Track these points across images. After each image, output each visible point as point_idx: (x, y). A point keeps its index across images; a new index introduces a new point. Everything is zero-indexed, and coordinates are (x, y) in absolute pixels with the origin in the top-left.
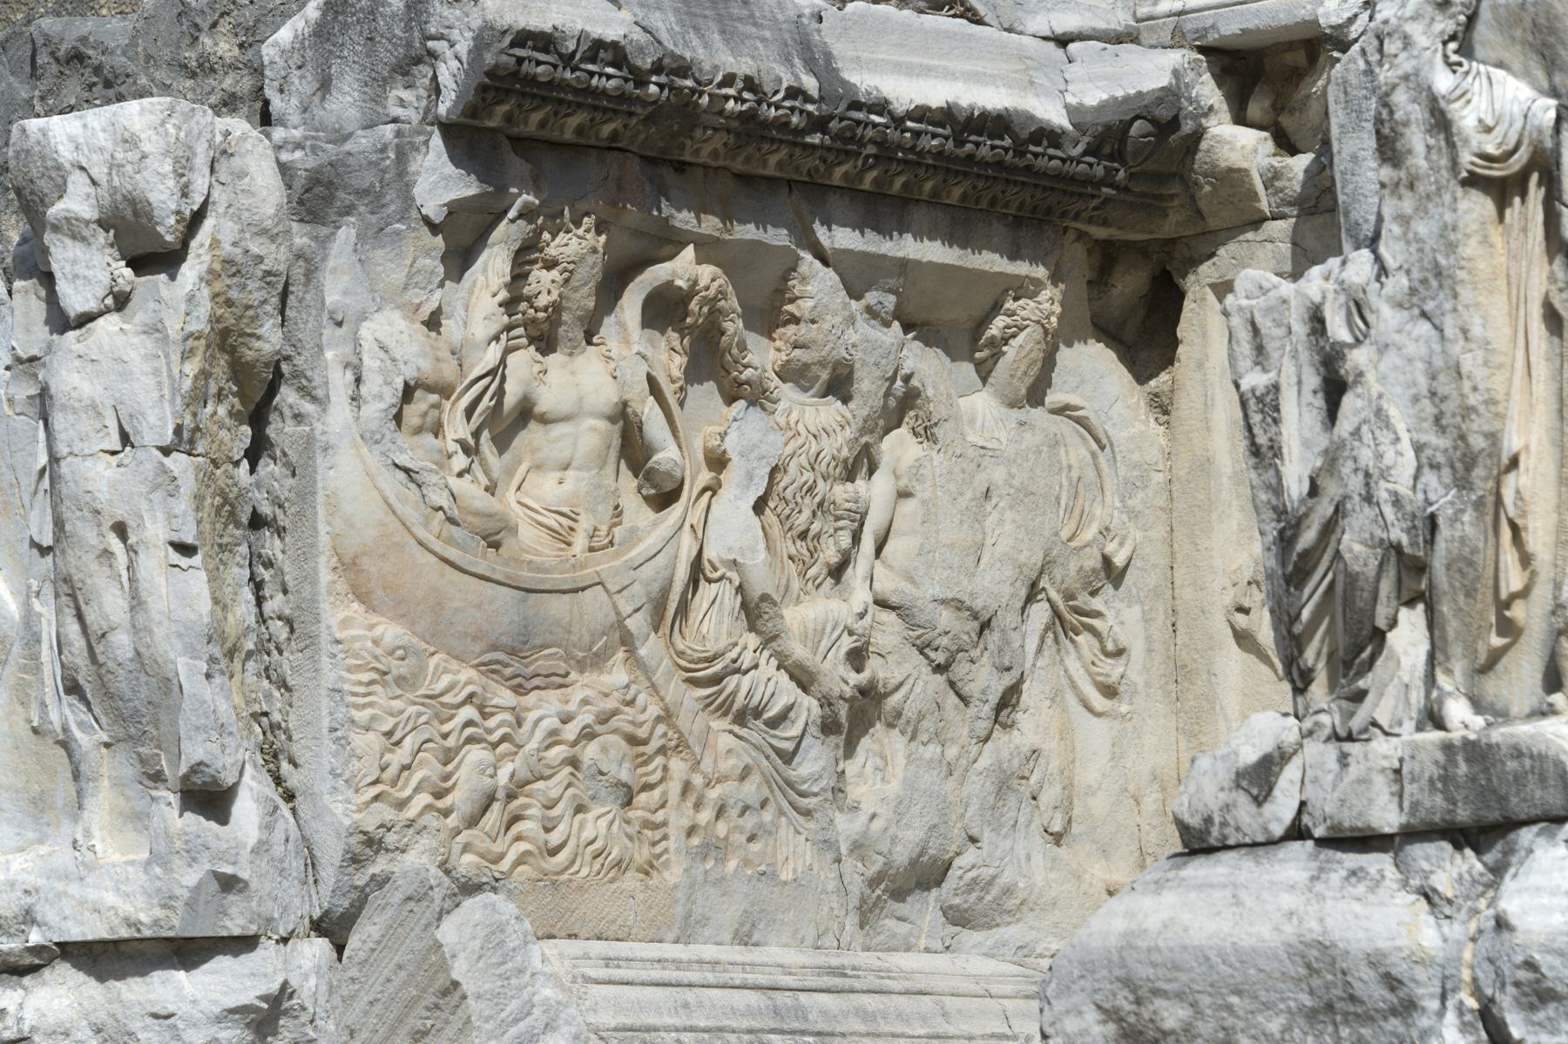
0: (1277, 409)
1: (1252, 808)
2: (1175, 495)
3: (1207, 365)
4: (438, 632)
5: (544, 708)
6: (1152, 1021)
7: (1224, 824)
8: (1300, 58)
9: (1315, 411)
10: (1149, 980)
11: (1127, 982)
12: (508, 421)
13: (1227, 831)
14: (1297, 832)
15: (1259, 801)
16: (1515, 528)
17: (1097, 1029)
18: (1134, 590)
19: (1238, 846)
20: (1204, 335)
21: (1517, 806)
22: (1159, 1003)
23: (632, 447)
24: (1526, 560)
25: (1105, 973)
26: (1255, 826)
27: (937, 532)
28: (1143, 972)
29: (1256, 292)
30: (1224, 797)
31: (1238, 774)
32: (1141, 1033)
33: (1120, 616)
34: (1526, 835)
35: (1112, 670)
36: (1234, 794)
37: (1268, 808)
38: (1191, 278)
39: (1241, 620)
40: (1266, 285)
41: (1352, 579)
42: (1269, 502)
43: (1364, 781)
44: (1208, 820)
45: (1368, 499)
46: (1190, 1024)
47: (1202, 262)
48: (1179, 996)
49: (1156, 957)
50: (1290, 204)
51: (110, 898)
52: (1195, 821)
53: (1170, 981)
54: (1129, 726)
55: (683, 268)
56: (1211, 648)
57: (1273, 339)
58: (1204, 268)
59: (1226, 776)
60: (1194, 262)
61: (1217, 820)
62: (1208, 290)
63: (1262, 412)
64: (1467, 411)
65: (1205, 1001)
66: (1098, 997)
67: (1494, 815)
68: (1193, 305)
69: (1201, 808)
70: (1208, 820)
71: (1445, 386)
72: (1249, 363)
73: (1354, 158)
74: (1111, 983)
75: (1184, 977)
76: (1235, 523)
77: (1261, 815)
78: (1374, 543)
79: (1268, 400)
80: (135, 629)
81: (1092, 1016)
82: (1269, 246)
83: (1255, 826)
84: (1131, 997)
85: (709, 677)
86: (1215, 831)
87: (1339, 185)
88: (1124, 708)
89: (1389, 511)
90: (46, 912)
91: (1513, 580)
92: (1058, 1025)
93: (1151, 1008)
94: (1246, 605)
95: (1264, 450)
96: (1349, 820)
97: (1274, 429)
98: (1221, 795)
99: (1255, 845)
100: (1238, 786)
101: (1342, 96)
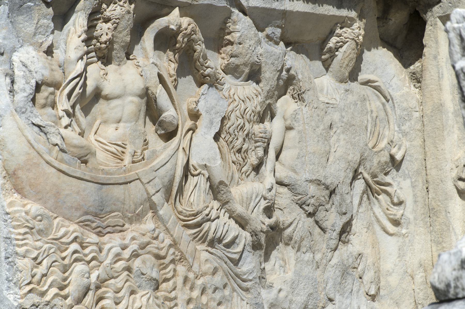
2: (425, 123)
3: (439, 57)
4: (58, 207)
5: (113, 242)
7: (456, 287)
12: (88, 100)
13: (458, 290)
18: (407, 172)
20: (437, 42)
23: (152, 110)
27: (306, 146)
29: (462, 19)
30: (455, 273)
33: (401, 185)
35: (397, 212)
36: (461, 272)
38: (429, 14)
44: (448, 286)
47: (434, 5)
52: (441, 286)
54: (407, 240)
55: (174, 19)
56: (446, 199)
58: (436, 9)
59: (456, 263)
60: (430, 6)
61: (453, 285)
62: (438, 19)
68: (431, 28)
69: (444, 279)
70: (448, 286)
72: (459, 55)
76: (456, 136)
85: (195, 224)
86: (452, 291)
88: (404, 231)
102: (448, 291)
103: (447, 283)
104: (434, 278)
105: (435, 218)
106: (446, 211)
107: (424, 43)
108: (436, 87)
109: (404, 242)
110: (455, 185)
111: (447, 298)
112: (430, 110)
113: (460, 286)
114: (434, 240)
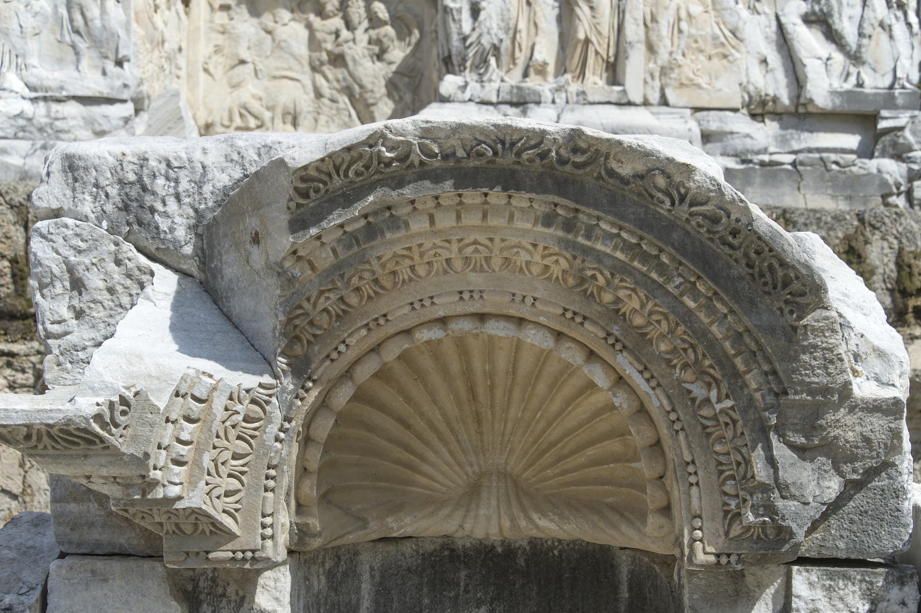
14: (470, 100)
15: (463, 92)
16: (520, 45)
21: (528, 99)
24: (521, 50)
33: (181, 60)
34: (530, 105)
35: (178, 72)
39: (206, 66)
41: (484, 49)
43: (490, 91)
45: (489, 33)
51: (93, 86)
64: (510, 19)
67: (522, 101)
70: (450, 96)
71: (505, 13)
78: (489, 43)
80: (102, 19)
89: (494, 37)
90: (66, 87)
91: (517, 54)
96: (486, 98)
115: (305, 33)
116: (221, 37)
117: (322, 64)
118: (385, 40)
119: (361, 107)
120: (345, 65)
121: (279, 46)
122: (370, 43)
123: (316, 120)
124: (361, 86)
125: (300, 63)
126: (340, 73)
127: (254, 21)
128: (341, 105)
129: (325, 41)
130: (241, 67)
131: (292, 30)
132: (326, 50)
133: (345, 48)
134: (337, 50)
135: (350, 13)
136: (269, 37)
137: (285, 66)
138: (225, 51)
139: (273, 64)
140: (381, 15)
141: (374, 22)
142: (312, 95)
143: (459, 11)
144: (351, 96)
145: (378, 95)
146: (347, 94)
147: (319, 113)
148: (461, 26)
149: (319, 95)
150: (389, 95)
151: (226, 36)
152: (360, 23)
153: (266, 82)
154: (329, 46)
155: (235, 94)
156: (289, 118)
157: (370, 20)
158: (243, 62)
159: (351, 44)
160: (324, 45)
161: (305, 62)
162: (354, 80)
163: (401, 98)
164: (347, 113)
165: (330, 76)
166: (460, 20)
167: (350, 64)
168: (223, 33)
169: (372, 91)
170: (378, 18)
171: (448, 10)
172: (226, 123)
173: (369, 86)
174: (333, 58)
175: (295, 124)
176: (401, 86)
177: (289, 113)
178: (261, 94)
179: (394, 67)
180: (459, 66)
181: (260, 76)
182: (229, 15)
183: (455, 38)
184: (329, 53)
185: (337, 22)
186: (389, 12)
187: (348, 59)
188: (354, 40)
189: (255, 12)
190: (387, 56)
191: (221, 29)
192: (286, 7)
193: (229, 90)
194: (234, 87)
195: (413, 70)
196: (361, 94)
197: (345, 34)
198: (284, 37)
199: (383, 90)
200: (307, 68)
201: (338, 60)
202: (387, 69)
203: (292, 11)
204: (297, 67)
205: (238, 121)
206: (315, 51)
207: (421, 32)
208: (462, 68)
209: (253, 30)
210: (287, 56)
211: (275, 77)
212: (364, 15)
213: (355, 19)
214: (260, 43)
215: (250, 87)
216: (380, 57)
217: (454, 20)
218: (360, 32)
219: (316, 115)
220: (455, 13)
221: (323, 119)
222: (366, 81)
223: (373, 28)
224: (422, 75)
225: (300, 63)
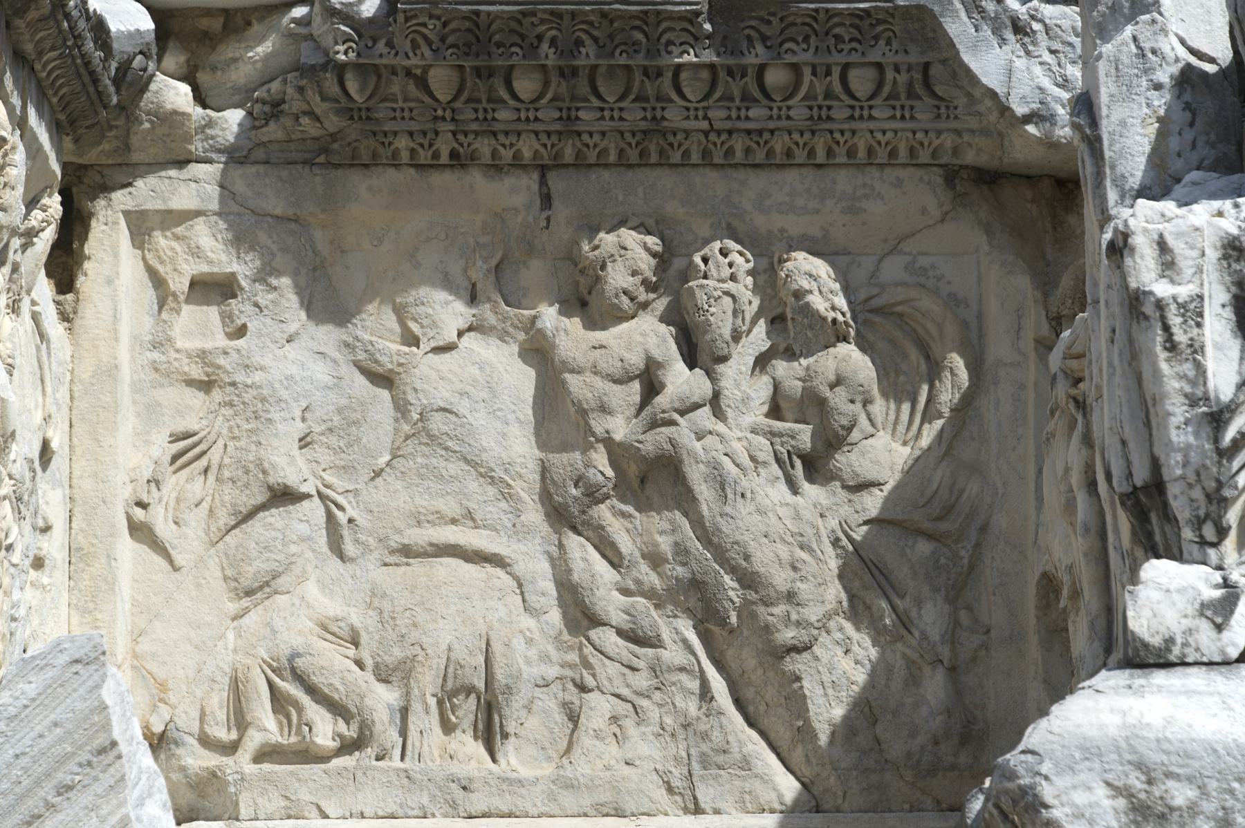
0: (1201, 315)
1: (1213, 634)
2: (76, 395)
3: (117, 282)
6: (1162, 798)
7: (1185, 645)
8: (216, 24)
9: (1224, 321)
10: (1163, 764)
11: (1140, 766)
13: (1187, 650)
15: (1219, 628)
17: (1107, 803)
18: (58, 475)
19: (1196, 663)
20: (116, 255)
22: (1171, 784)
25: (1114, 756)
26: (1213, 648)
28: (1155, 757)
29: (1157, 218)
30: (1186, 623)
31: (1202, 605)
32: (1149, 807)
36: (1197, 621)
37: (1226, 635)
38: (101, 203)
39: (139, 513)
40: (1169, 214)
42: (1181, 389)
44: (1170, 641)
46: (1195, 803)
47: (114, 189)
48: (1190, 779)
49: (1166, 746)
50: (219, 151)
53: (1182, 766)
54: (48, 597)
56: (112, 535)
57: (1186, 258)
58: (118, 196)
60: (106, 188)
61: (1179, 640)
62: (121, 215)
63: (1183, 315)
65: (1213, 784)
66: (1110, 777)
68: (104, 227)
69: (1162, 629)
70: (1170, 641)
72: (1153, 275)
73: (1123, 123)
74: (1122, 764)
75: (1196, 764)
76: (130, 426)
77: (1220, 639)
79: (1192, 306)
81: (1101, 792)
82: (193, 185)
83: (1213, 648)
84: (1143, 778)
86: (1176, 650)
87: (1106, 143)
88: (45, 580)
92: (1064, 798)
93: (1163, 787)
94: (146, 501)
95: (1183, 346)
97: (1196, 331)
98: (1184, 621)
99: (1211, 664)
100: (1202, 615)
101: (1113, 71)
102: (1169, 650)
103: (1167, 636)
104: (1142, 626)
105: (81, 565)
106: (108, 556)
107: (87, 252)
108: (107, 334)
109: (44, 599)
110: (127, 513)
111: (1162, 661)
112: (89, 374)
113: (1193, 644)
114: (76, 605)
115: (520, 380)
116: (196, 399)
117: (593, 496)
118: (838, 399)
119: (747, 659)
120: (685, 500)
121: (421, 428)
122: (775, 411)
123: (574, 718)
124: (748, 580)
125: (507, 495)
126: (664, 529)
127: (326, 336)
128: (672, 655)
129: (604, 409)
130: (275, 517)
131: (478, 373)
132: (608, 442)
133: (683, 432)
134: (652, 443)
135: (701, 298)
136: (385, 394)
137: (450, 507)
138: (215, 455)
139: (391, 504)
140: (819, 303)
141: (792, 328)
142: (555, 616)
143: (1193, 311)
144: (708, 619)
145: (813, 613)
146: (689, 612)
147: (583, 688)
148: (1201, 370)
149: (580, 615)
150: (858, 610)
151: (217, 395)
152: (737, 336)
153: (372, 571)
154: (620, 427)
155: (252, 620)
156: (468, 708)
157: (777, 322)
158: (284, 496)
159: (704, 416)
160: (599, 425)
161: (526, 490)
162: (720, 555)
163: (904, 621)
164: (694, 685)
165: (626, 544)
166: (1197, 348)
167: (704, 492)
168: (206, 386)
169: (790, 596)
170: (807, 310)
171: (1148, 309)
172: (222, 734)
173: (781, 579)
174: (633, 470)
175: (490, 734)
176: (902, 573)
177: (469, 690)
178: (356, 617)
179: (872, 503)
180: (1199, 523)
181: (350, 548)
182: (227, 317)
183: (1177, 411)
184: (616, 452)
185: (647, 335)
186: (847, 290)
187: (695, 474)
188: (715, 401)
189: (328, 303)
190: (849, 461)
191: (197, 372)
192: (447, 283)
193: (232, 607)
194: (249, 593)
195: (947, 512)
196: (746, 610)
197: (681, 380)
198: (442, 395)
199: (835, 592)
200: (534, 515)
201: (655, 478)
202: (846, 511)
203: (473, 299)
204: (495, 511)
205: (267, 726)
206: (564, 447)
207: (975, 368)
208: (1209, 532)
209: (320, 372)
210: (455, 467)
211: (407, 552)
212: (751, 303)
213: (721, 320)
214: (349, 421)
215: (312, 590)
216: (816, 464)
217: (1171, 346)
218: (736, 373)
219: (572, 694)
220: (1175, 320)
221: (598, 708)
222: (768, 559)
223: (790, 355)
224: (984, 529)
225: (507, 495)
